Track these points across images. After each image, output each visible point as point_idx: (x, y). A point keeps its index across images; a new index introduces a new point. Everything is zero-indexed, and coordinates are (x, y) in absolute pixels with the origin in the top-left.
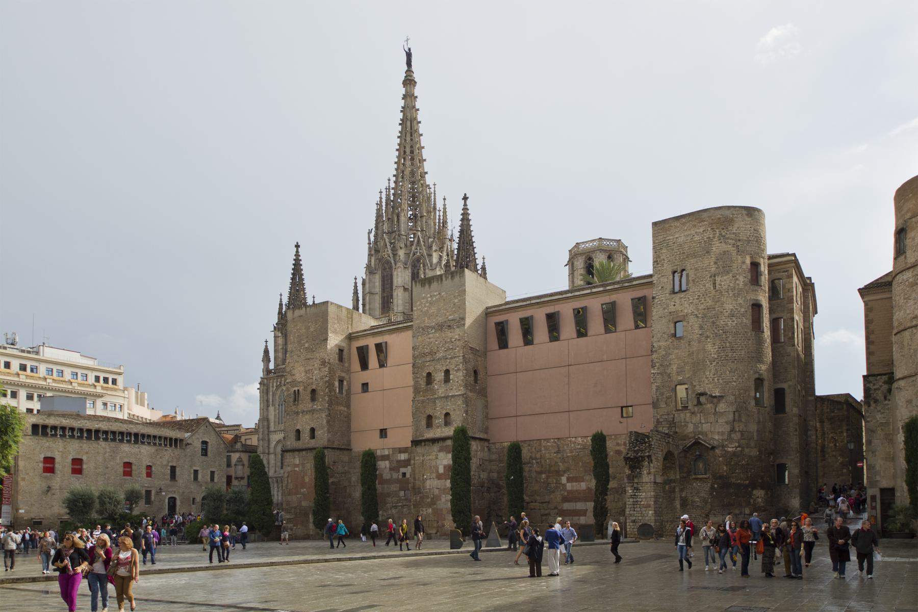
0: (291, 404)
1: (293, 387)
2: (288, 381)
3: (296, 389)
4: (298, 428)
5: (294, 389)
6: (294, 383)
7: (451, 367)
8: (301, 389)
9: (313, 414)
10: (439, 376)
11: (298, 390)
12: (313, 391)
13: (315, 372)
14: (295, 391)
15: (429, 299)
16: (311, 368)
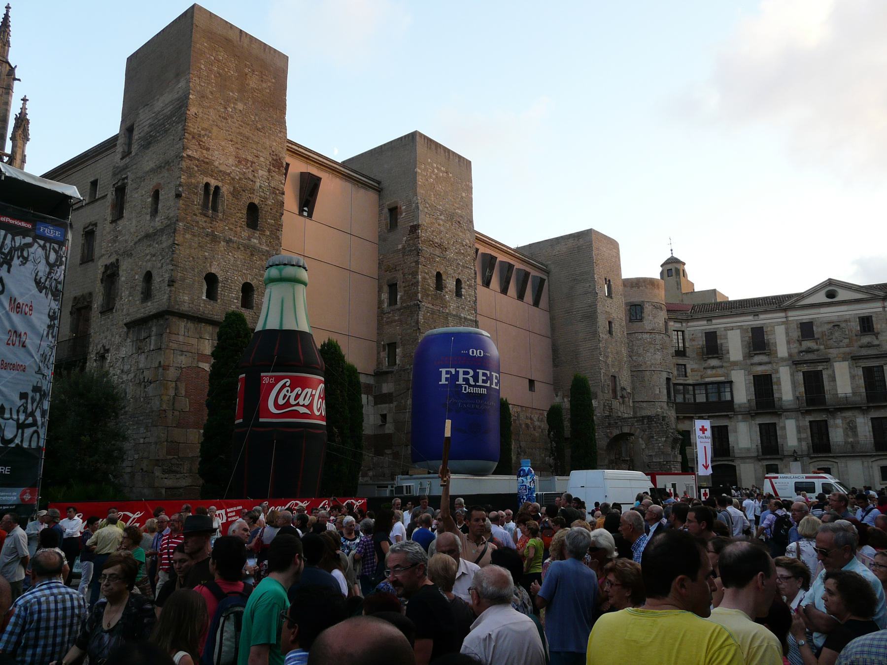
0: (197, 208)
1: (205, 173)
2: (190, 153)
3: (213, 183)
4: (213, 271)
5: (206, 179)
6: (206, 166)
7: (463, 278)
8: (225, 189)
9: (252, 255)
10: (451, 284)
11: (217, 188)
12: (253, 210)
13: (261, 172)
14: (207, 185)
15: (436, 171)
16: (250, 158)
